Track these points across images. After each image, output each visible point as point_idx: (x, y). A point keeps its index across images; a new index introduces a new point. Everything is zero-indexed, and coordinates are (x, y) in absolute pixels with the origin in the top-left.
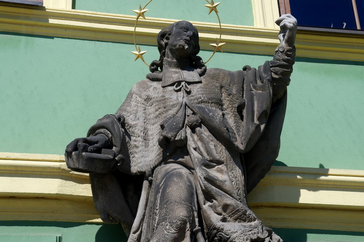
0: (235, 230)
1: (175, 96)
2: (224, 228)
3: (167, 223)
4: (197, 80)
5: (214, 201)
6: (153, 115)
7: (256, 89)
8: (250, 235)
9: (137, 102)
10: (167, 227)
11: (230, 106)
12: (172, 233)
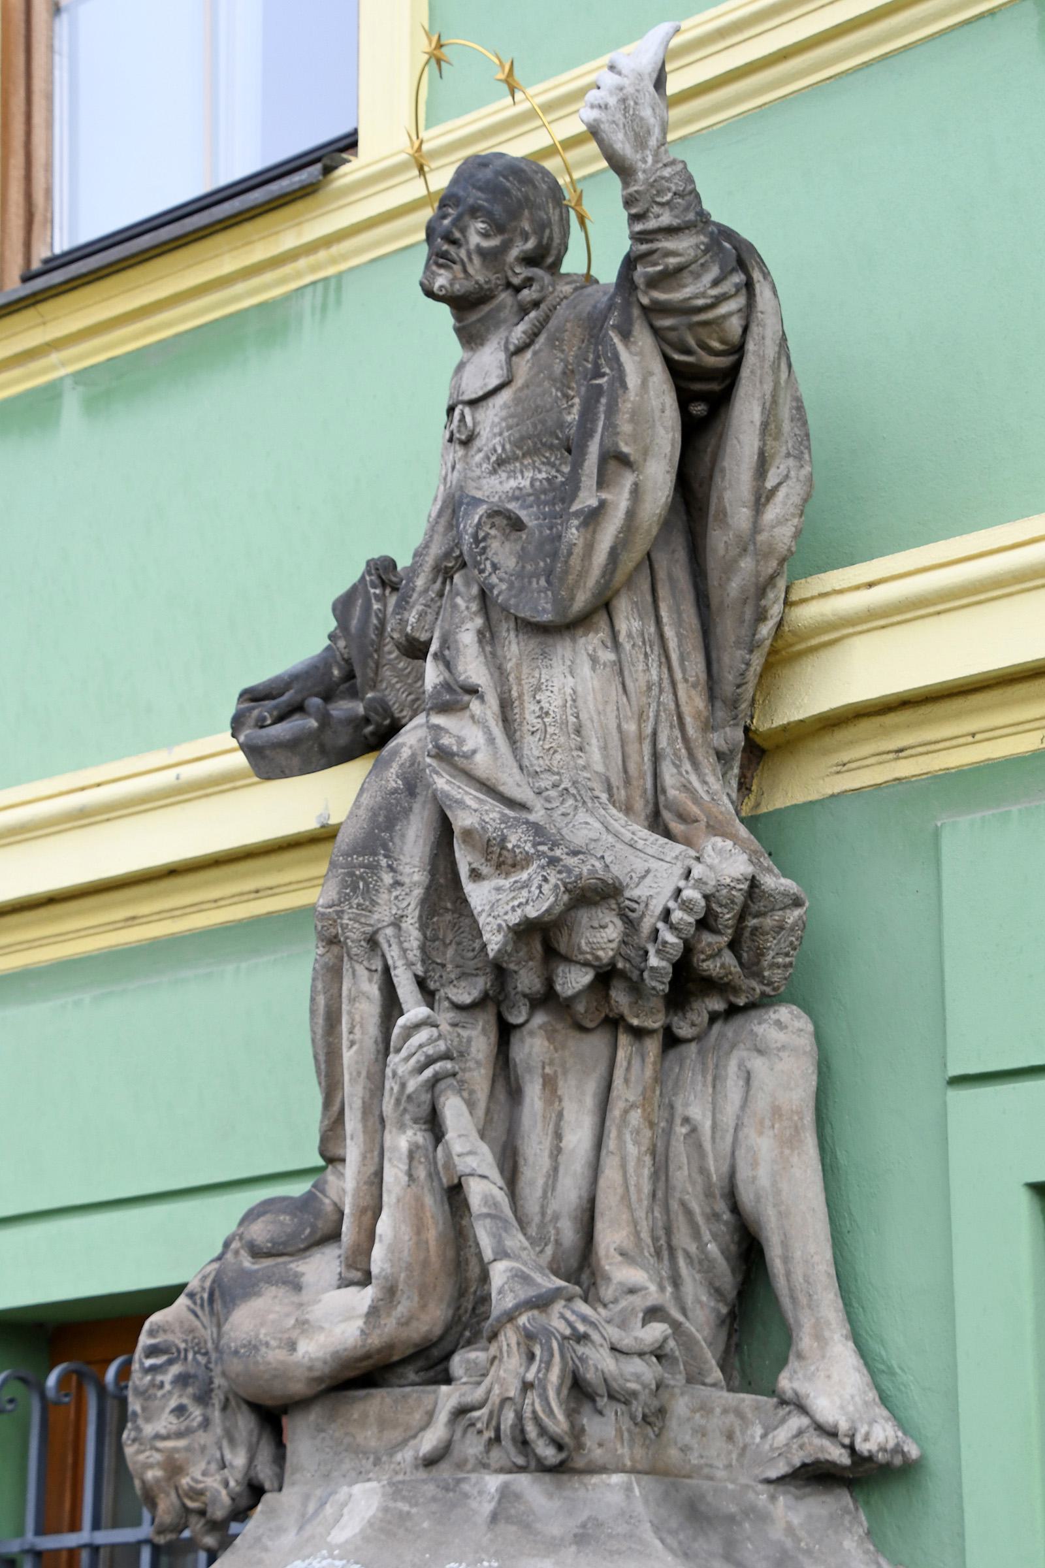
4: (494, 382)
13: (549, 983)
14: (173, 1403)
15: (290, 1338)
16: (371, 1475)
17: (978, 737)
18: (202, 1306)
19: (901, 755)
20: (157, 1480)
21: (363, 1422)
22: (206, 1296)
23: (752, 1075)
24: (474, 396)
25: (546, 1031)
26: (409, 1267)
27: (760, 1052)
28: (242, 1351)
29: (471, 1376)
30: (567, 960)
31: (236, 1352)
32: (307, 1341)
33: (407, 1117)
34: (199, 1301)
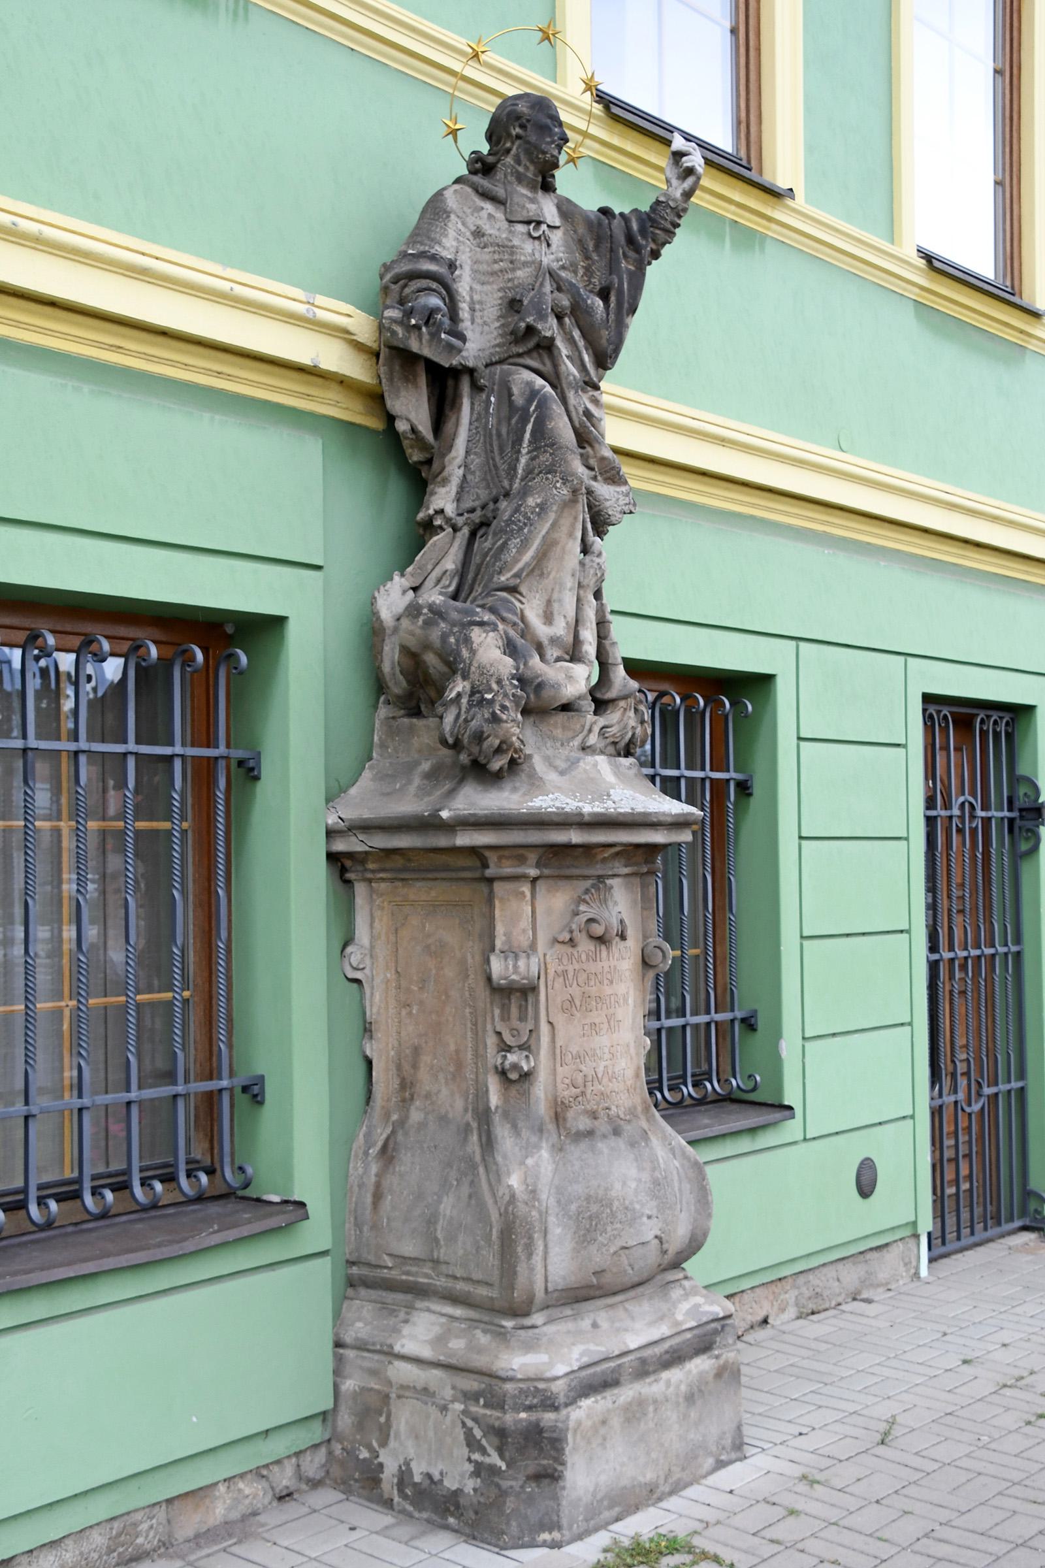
1: (529, 247)
3: (558, 479)
5: (589, 449)
6: (485, 267)
7: (628, 262)
9: (459, 232)
10: (558, 485)
11: (586, 278)
24: (552, 224)
31: (553, 686)
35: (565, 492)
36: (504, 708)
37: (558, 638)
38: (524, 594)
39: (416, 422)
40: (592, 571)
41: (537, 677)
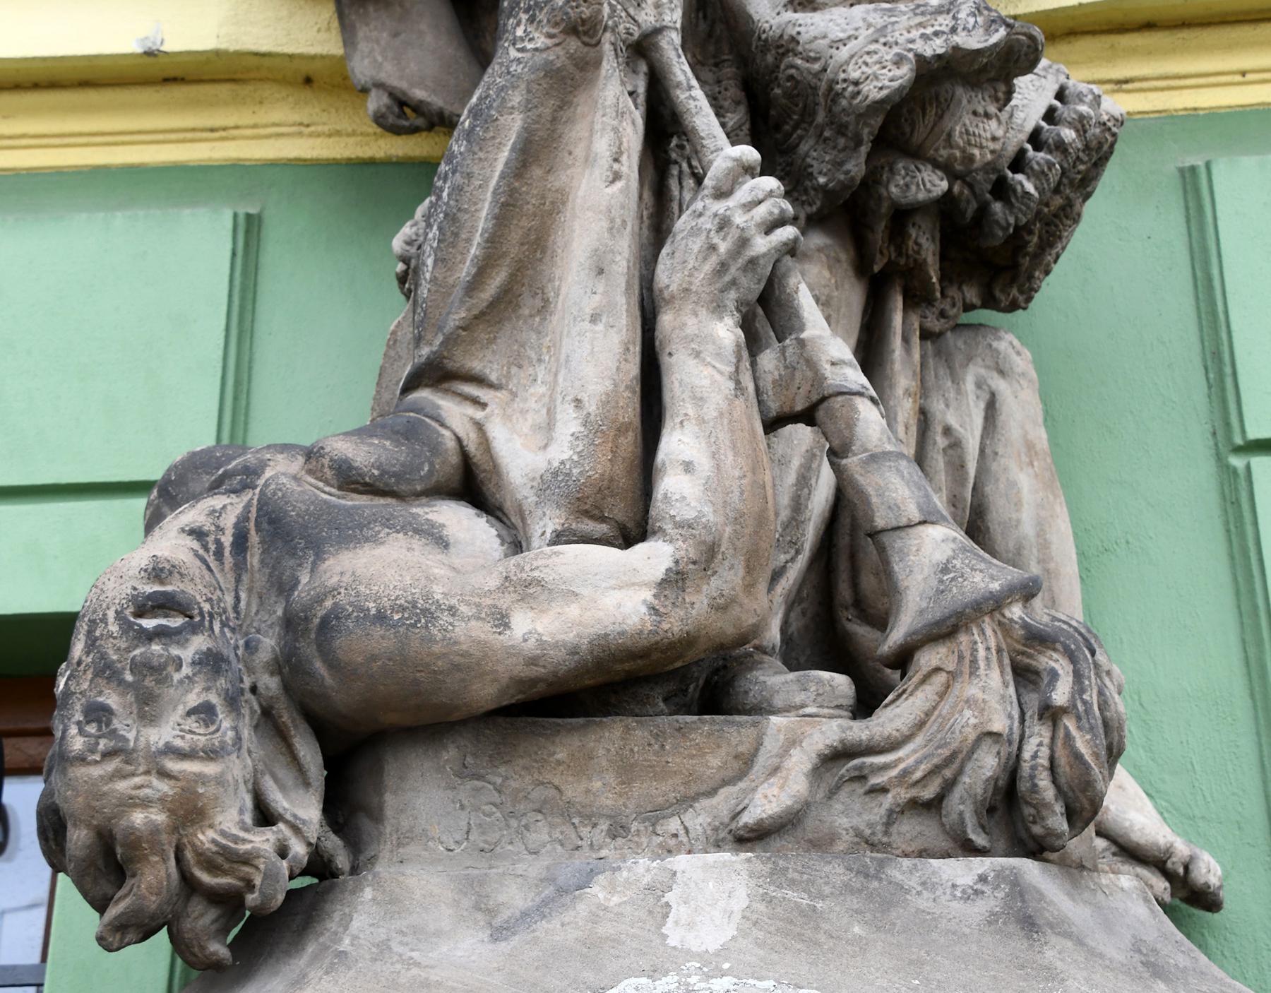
0: (844, 31)
2: (799, 33)
8: (912, 41)
12: (536, 49)
13: (871, 182)
14: (194, 699)
15: (495, 606)
16: (604, 853)
17: (1249, 77)
18: (219, 554)
19: (1125, 86)
20: (155, 830)
21: (582, 766)
22: (227, 540)
23: (997, 397)
25: (828, 257)
26: (738, 519)
27: (1002, 373)
28: (396, 617)
29: (821, 706)
30: (917, 154)
32: (531, 614)
33: (733, 295)
34: (212, 547)
35: (541, 41)
36: (98, 714)
37: (555, 474)
38: (493, 377)
39: (402, 85)
40: (697, 244)
41: (319, 600)
